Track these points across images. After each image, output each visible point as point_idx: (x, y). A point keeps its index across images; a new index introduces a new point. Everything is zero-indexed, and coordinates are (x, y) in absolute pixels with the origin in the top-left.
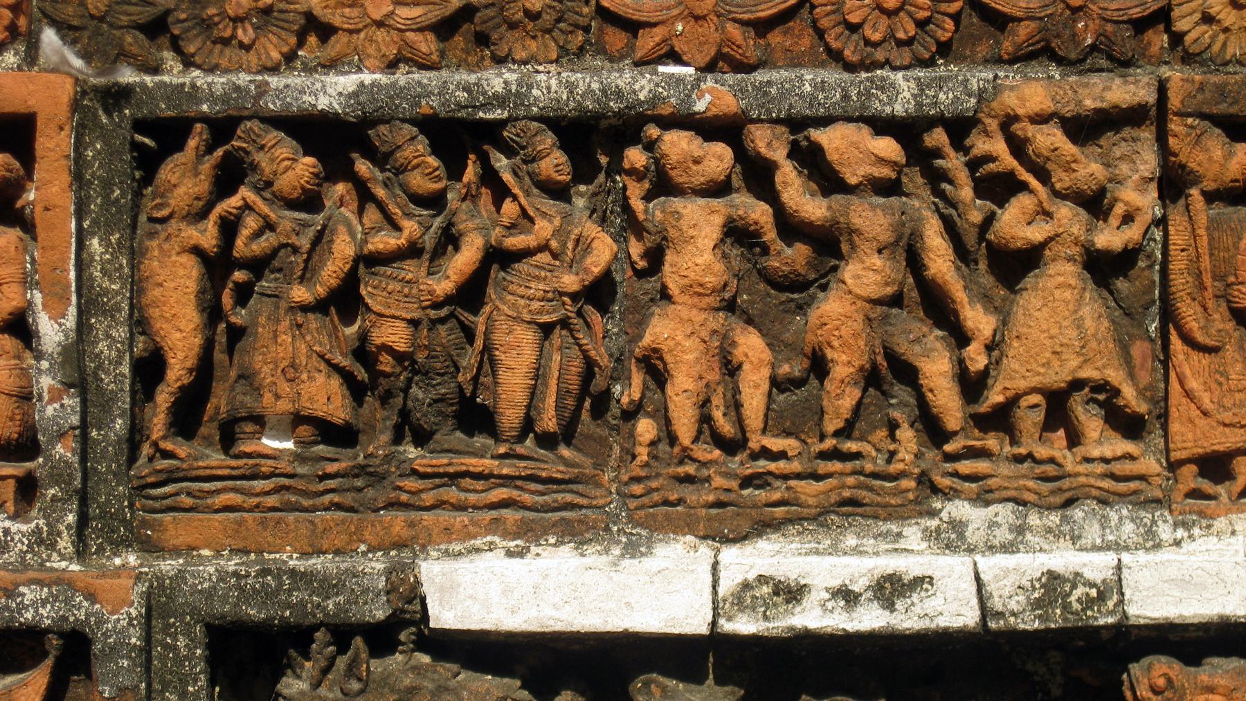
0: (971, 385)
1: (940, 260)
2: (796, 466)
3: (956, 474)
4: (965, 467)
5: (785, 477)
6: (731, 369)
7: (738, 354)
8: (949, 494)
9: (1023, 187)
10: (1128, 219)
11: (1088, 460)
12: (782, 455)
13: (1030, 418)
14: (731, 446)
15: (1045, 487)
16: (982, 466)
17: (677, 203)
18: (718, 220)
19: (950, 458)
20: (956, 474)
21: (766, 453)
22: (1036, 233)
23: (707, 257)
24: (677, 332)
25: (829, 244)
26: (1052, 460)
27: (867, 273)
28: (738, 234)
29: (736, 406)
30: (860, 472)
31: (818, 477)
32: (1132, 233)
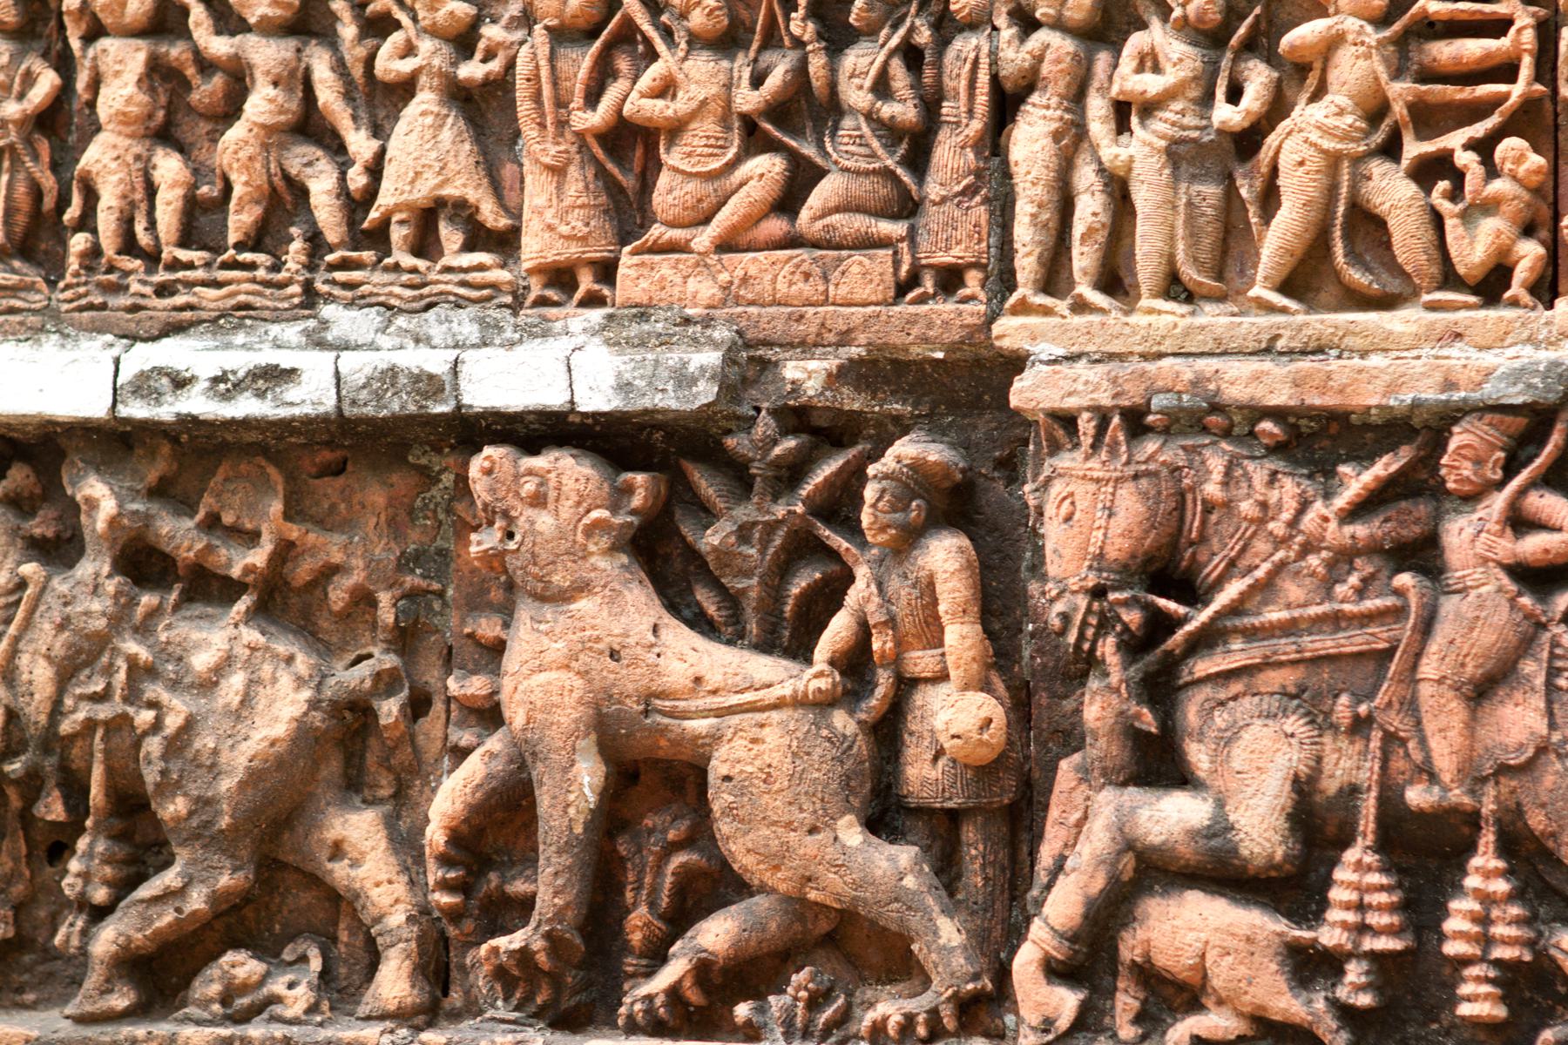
0: (355, 204)
1: (328, 93)
2: (200, 274)
3: (334, 282)
4: (340, 276)
5: (189, 284)
6: (151, 190)
7: (157, 176)
8: (330, 298)
9: (398, 25)
10: (489, 56)
11: (448, 269)
12: (190, 266)
13: (398, 234)
14: (152, 258)
15: (408, 293)
16: (356, 275)
17: (104, 43)
18: (142, 57)
19: (332, 267)
20: (334, 282)
21: (175, 265)
22: (407, 66)
23: (131, 89)
24: (104, 158)
25: (239, 79)
26: (414, 270)
27: (262, 104)
28: (158, 73)
29: (152, 225)
30: (254, 281)
31: (218, 284)
32: (495, 66)
